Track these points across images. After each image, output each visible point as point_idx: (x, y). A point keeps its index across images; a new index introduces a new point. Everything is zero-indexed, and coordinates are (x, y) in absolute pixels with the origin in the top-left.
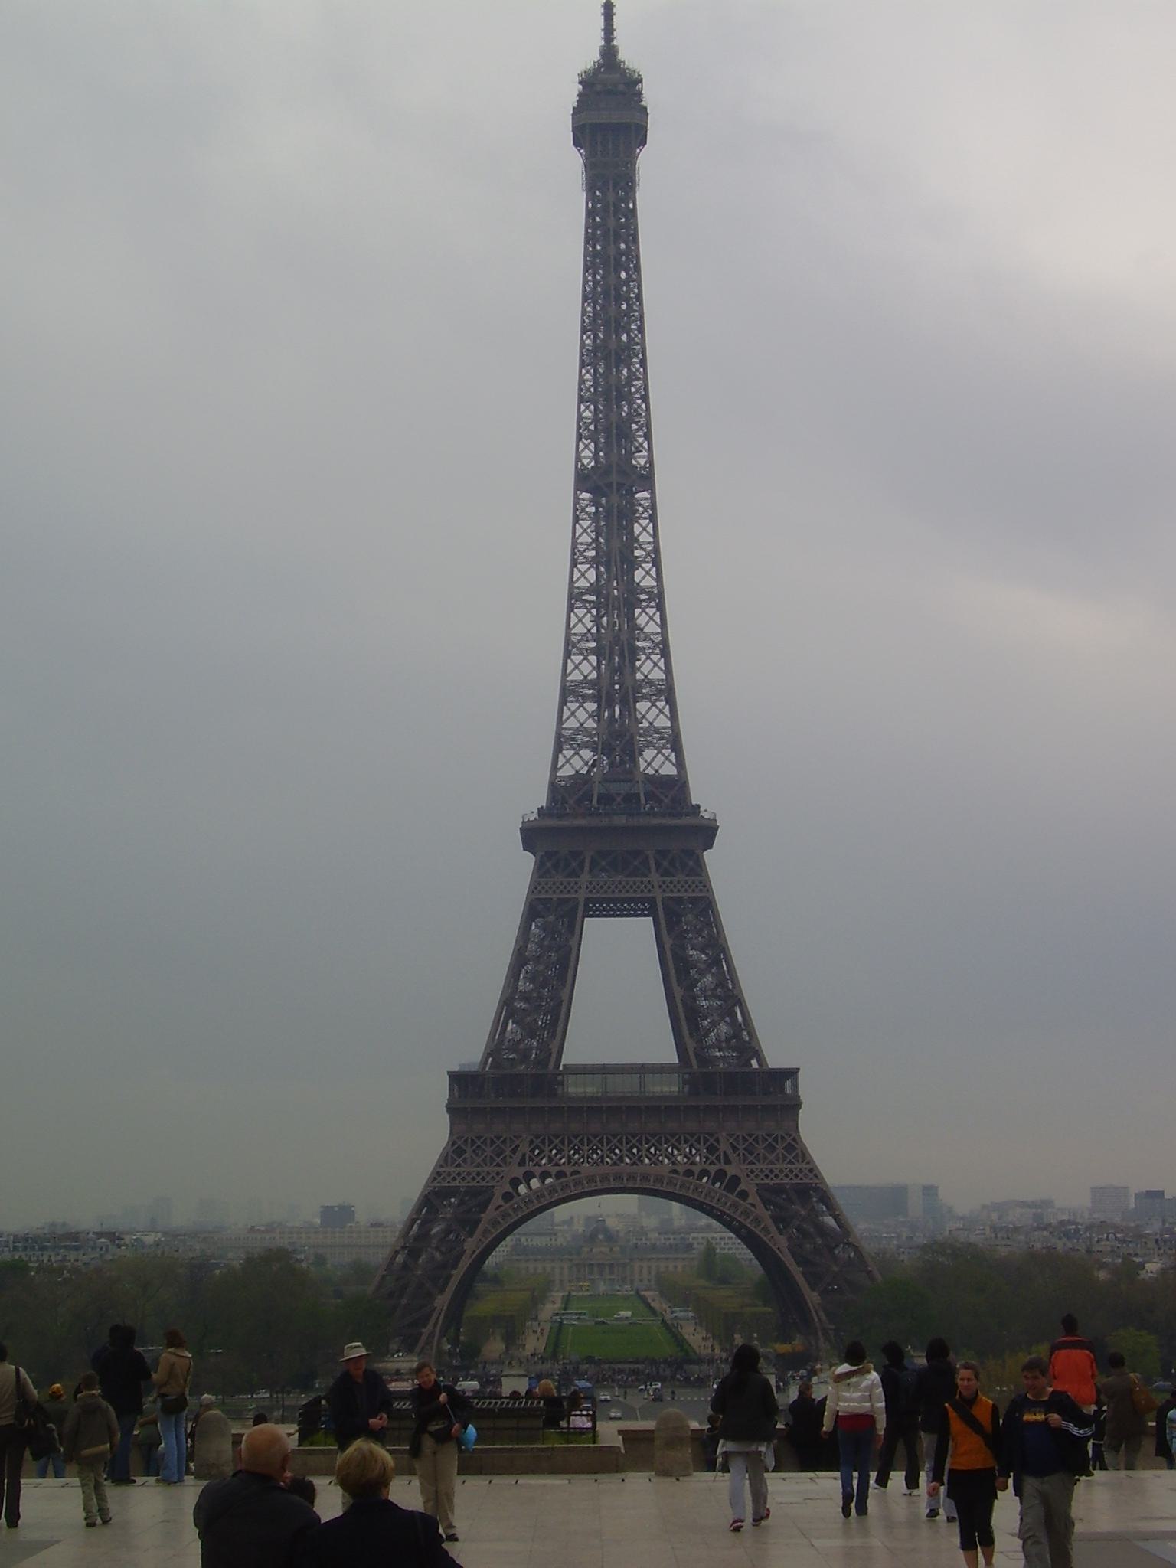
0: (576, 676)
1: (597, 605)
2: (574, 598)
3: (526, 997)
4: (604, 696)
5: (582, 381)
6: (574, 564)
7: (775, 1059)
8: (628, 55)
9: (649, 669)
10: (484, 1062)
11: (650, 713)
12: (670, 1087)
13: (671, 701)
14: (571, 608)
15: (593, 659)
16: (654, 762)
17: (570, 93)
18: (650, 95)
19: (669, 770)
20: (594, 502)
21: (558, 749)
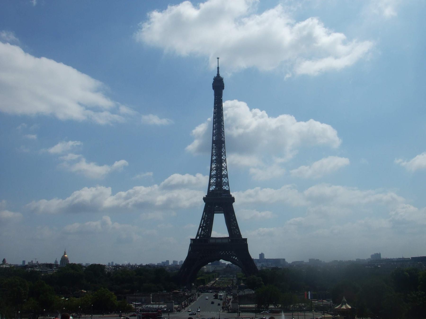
0: (212, 174)
1: (216, 162)
2: (212, 161)
3: (204, 226)
4: (217, 178)
5: (213, 126)
6: (212, 156)
7: (243, 237)
8: (221, 75)
9: (223, 173)
10: (197, 237)
11: (224, 180)
12: (226, 241)
13: (227, 178)
14: (211, 163)
15: (215, 171)
16: (225, 188)
17: (212, 81)
18: (225, 81)
19: (227, 189)
20: (215, 146)
21: (210, 185)
